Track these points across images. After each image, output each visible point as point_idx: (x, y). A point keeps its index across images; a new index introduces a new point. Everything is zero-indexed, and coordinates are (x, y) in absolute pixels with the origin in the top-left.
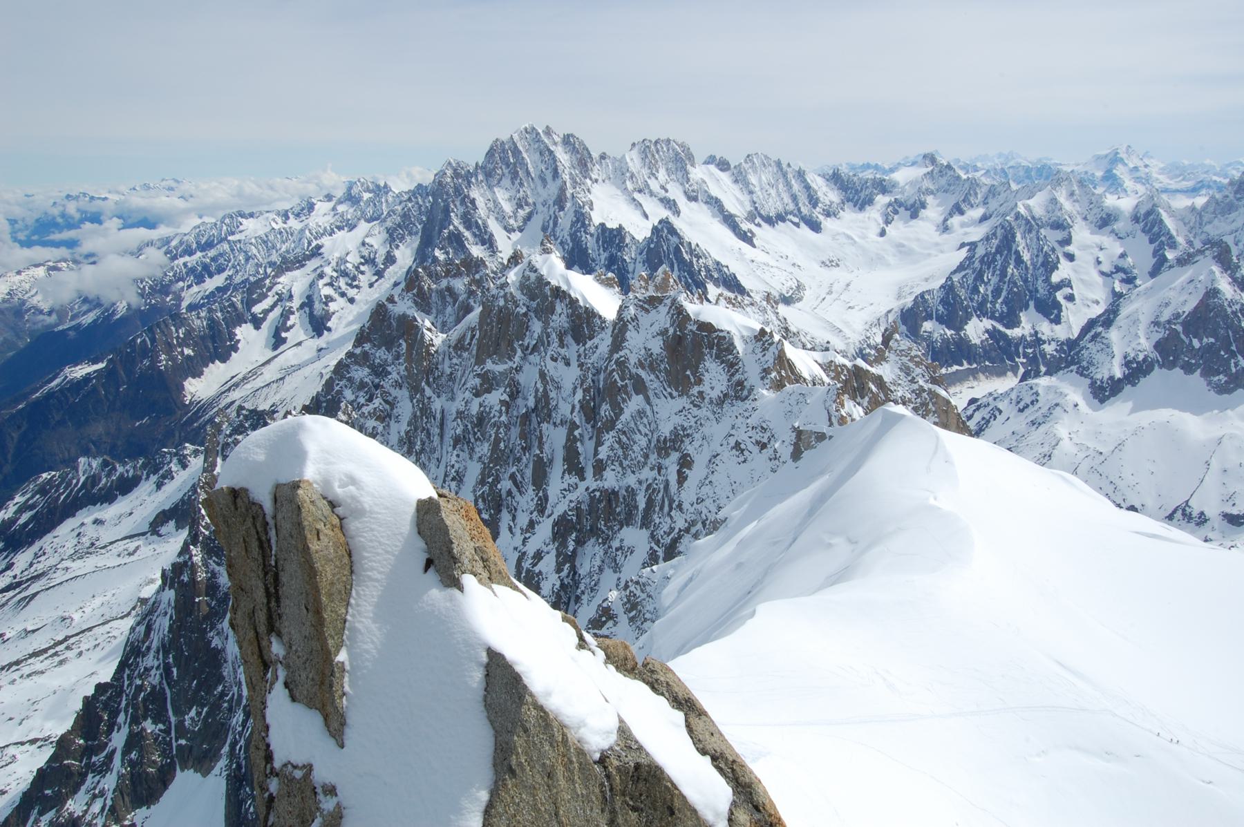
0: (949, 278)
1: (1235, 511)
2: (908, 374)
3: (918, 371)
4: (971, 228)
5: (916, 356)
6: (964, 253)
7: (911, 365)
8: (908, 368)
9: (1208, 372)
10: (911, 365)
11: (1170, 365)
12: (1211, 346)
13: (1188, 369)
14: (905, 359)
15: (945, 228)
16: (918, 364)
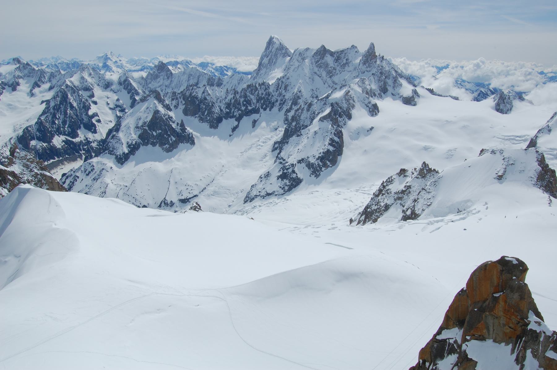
0: (39, 119)
1: (183, 198)
2: (28, 168)
3: (33, 165)
4: (45, 93)
5: (30, 159)
6: (44, 106)
7: (28, 163)
8: (27, 165)
9: (161, 145)
10: (28, 163)
11: (146, 144)
12: (160, 134)
13: (154, 144)
14: (25, 161)
15: (32, 95)
16: (32, 162)
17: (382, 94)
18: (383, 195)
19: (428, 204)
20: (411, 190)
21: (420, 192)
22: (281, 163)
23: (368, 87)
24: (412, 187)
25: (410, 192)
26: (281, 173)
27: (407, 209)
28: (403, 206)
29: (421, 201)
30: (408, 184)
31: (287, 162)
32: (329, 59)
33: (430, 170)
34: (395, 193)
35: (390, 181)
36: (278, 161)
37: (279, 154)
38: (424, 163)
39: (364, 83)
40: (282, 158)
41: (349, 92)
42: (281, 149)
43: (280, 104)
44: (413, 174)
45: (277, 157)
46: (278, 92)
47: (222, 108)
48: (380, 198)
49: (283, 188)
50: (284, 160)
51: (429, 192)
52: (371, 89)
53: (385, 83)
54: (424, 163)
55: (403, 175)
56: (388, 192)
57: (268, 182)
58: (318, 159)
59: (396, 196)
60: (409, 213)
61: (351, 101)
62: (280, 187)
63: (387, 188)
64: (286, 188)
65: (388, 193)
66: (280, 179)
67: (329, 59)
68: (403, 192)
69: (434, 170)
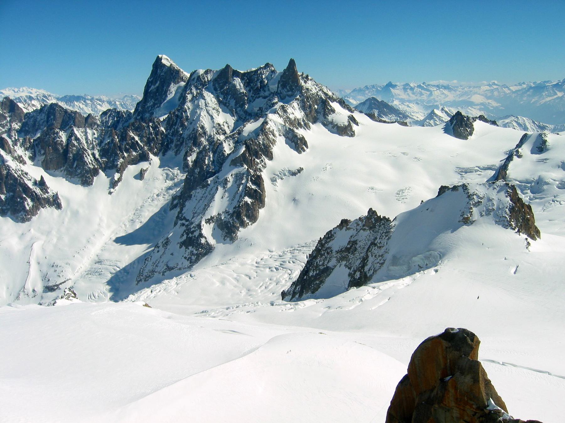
17: (311, 124)
18: (322, 255)
19: (382, 261)
20: (357, 246)
21: (369, 247)
22: (183, 225)
23: (292, 117)
24: (358, 242)
25: (356, 249)
26: (185, 237)
27: (355, 272)
28: (350, 268)
29: (371, 259)
30: (352, 239)
31: (192, 223)
32: (238, 83)
33: (379, 219)
34: (337, 252)
35: (330, 236)
36: (180, 222)
37: (180, 212)
39: (285, 111)
40: (185, 218)
41: (266, 123)
42: (183, 206)
43: (176, 146)
44: (358, 225)
45: (178, 217)
46: (172, 130)
47: (97, 156)
48: (318, 260)
49: (189, 259)
50: (187, 220)
51: (380, 247)
52: (295, 119)
55: (345, 228)
56: (329, 251)
57: (168, 252)
58: (232, 215)
59: (339, 255)
60: (358, 275)
62: (185, 258)
63: (326, 246)
64: (194, 258)
65: (328, 253)
66: (184, 247)
67: (238, 83)
68: (347, 250)
69: (384, 217)
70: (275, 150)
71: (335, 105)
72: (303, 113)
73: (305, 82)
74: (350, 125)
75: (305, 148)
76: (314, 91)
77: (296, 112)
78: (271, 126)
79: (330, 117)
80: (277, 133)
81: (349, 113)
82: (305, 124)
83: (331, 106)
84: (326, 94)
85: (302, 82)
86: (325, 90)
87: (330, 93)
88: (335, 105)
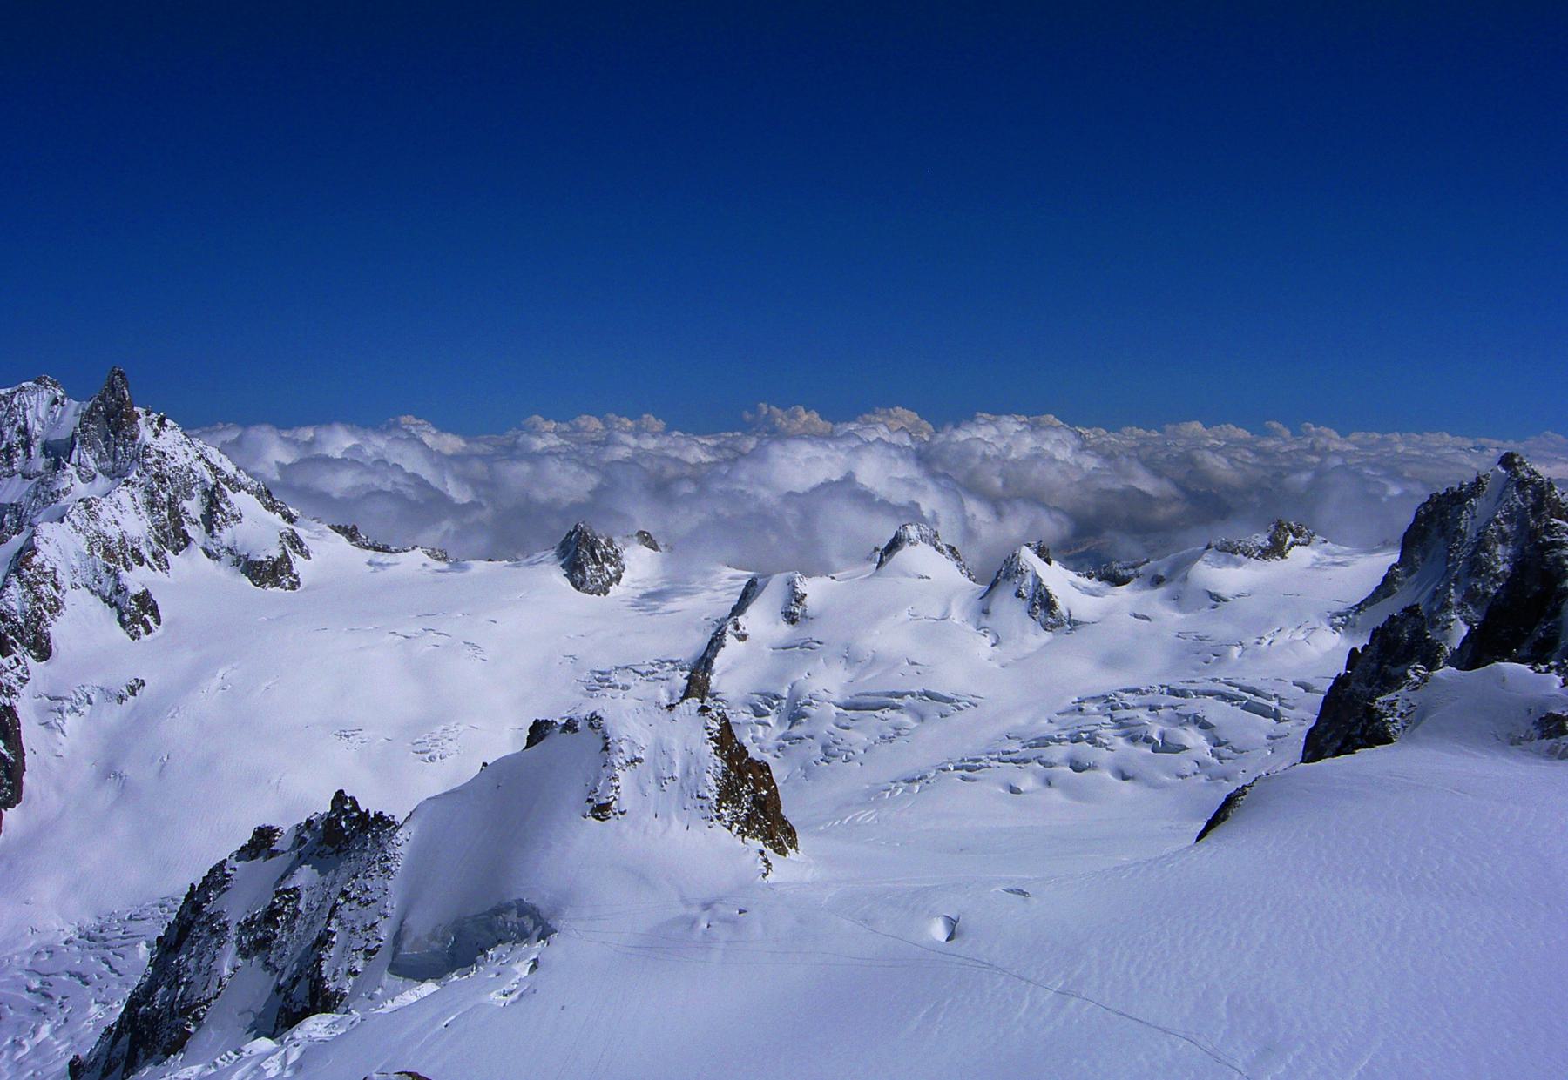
38: (340, 795)
39: (94, 517)
41: (29, 549)
53: (177, 515)
54: (340, 795)
61: (46, 589)
70: (59, 630)
71: (243, 501)
72: (147, 522)
73: (157, 435)
74: (285, 558)
75: (152, 624)
76: (181, 461)
77: (127, 516)
78: (46, 554)
79: (226, 535)
80: (65, 579)
81: (285, 525)
82: (155, 556)
83: (229, 504)
84: (215, 470)
85: (146, 435)
86: (215, 460)
87: (229, 468)
88: (243, 501)
